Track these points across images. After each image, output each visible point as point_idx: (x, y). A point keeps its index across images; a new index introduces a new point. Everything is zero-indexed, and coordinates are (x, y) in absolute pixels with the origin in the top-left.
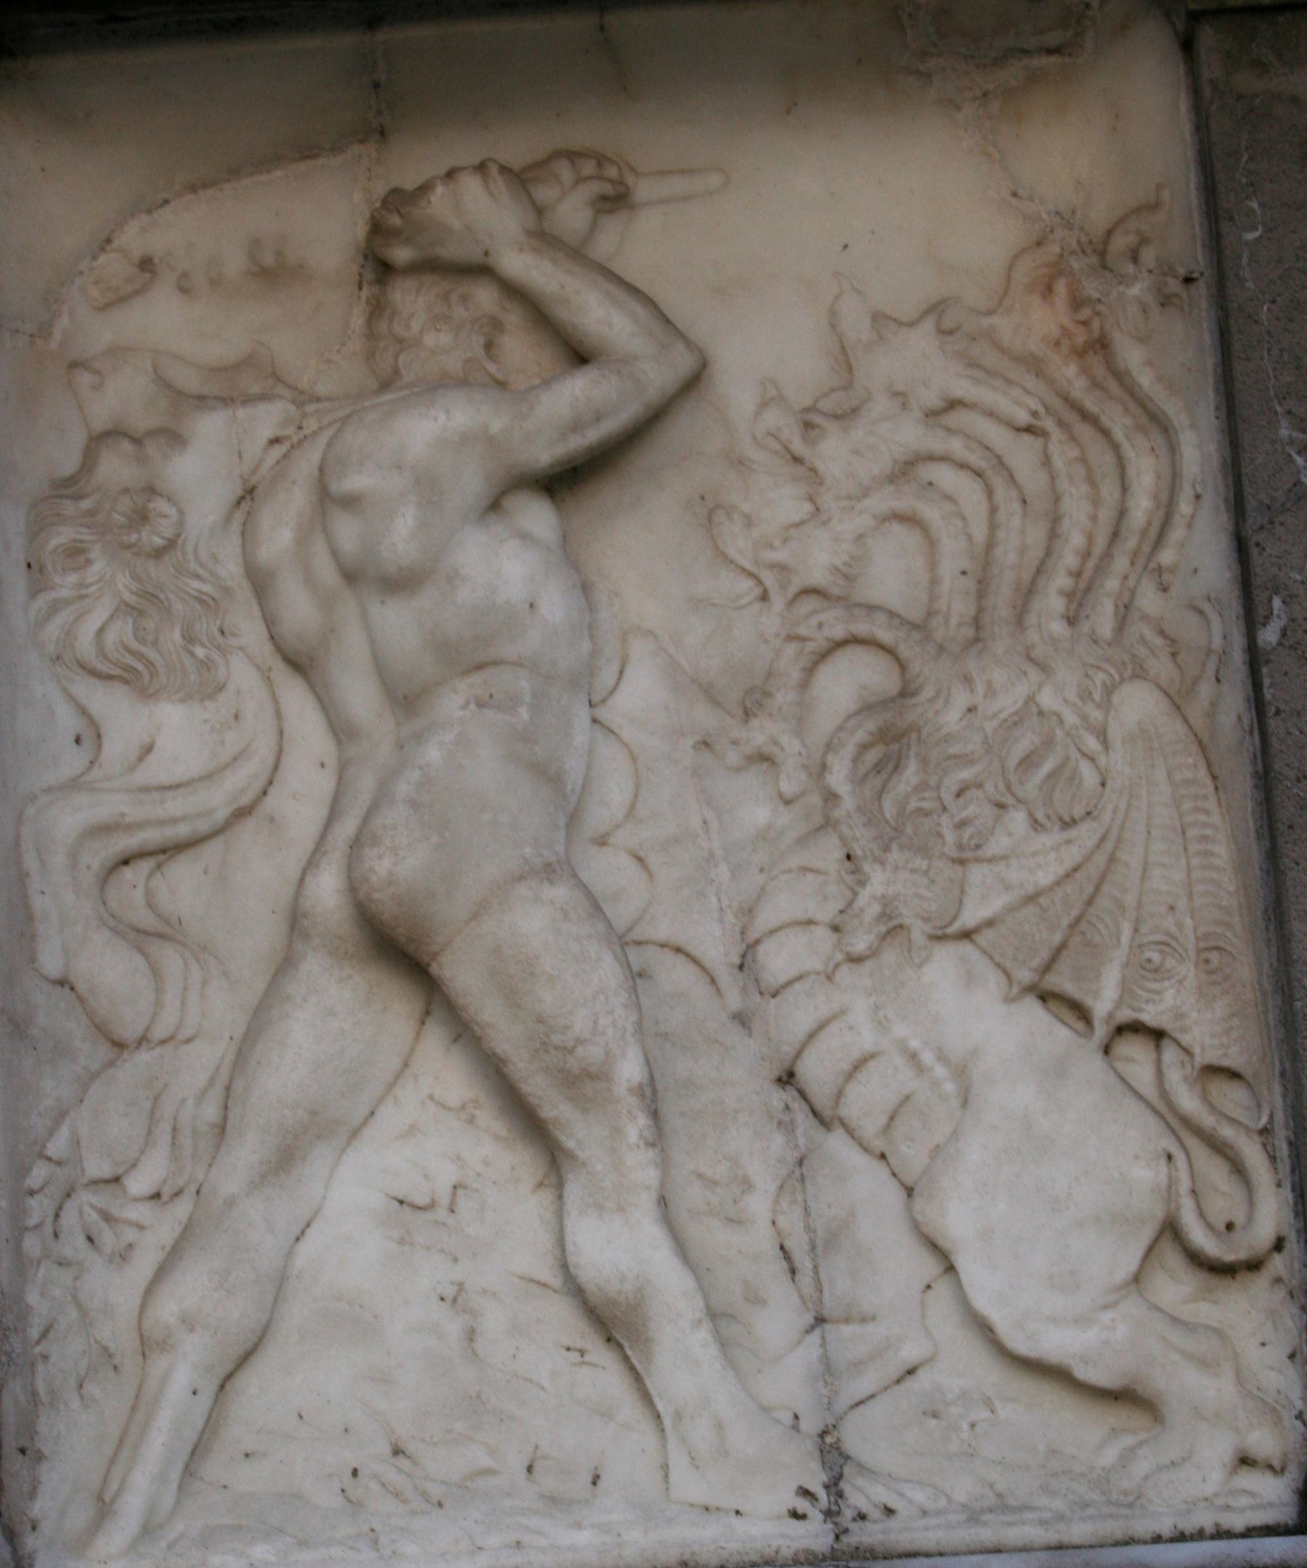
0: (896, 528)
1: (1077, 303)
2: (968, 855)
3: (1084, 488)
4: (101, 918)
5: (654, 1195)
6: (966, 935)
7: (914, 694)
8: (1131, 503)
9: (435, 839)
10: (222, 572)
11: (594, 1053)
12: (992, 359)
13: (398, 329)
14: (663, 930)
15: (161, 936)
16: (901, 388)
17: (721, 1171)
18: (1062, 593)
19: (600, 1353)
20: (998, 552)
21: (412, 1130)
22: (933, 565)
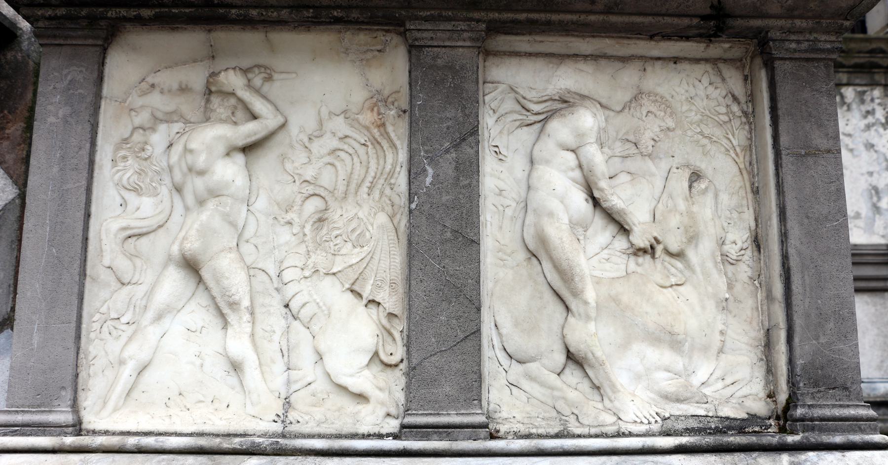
0: (329, 166)
1: (379, 114)
2: (336, 253)
3: (376, 161)
4: (122, 251)
5: (249, 335)
6: (334, 274)
7: (328, 210)
8: (386, 166)
9: (202, 240)
10: (161, 164)
11: (236, 298)
12: (357, 125)
13: (211, 106)
14: (260, 266)
15: (136, 256)
16: (334, 131)
17: (268, 328)
18: (367, 187)
19: (232, 373)
20: (353, 175)
21: (193, 311)
22: (337, 176)
